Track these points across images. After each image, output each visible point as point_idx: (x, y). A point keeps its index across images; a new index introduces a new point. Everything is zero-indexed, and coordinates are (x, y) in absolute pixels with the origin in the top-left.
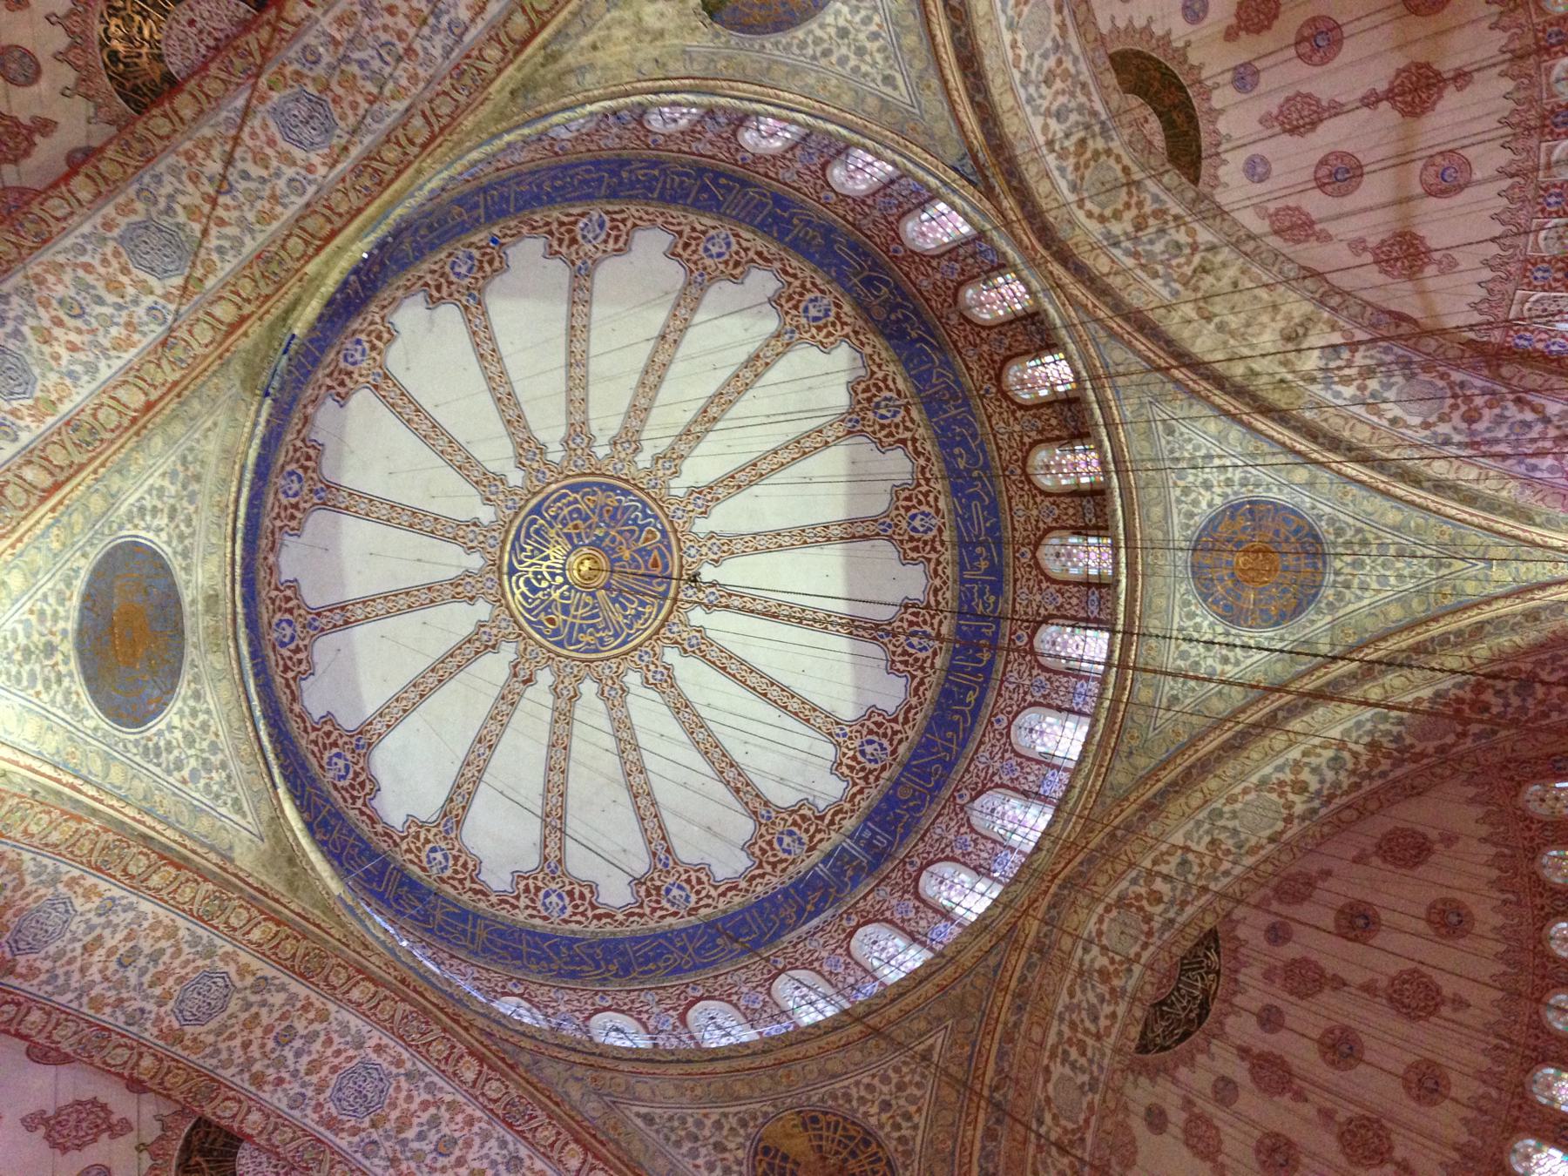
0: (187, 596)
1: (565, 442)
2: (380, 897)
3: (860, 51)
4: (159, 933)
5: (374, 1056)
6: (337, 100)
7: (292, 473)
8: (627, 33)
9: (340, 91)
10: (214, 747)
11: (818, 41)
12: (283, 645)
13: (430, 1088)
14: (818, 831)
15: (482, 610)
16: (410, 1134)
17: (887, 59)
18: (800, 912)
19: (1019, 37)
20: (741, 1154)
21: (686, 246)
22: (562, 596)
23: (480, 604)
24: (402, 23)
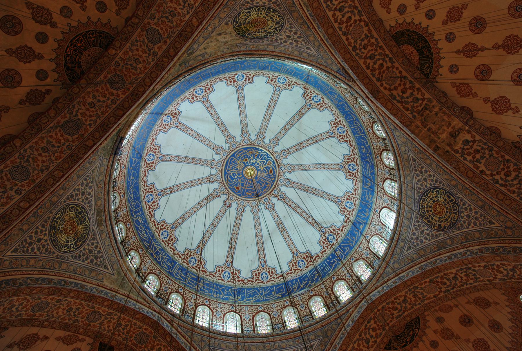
2: (170, 273)
4: (77, 304)
6: (125, 75)
9: (126, 73)
10: (99, 252)
11: (281, 39)
12: (149, 202)
13: (159, 340)
17: (306, 43)
19: (349, 37)
24: (141, 53)
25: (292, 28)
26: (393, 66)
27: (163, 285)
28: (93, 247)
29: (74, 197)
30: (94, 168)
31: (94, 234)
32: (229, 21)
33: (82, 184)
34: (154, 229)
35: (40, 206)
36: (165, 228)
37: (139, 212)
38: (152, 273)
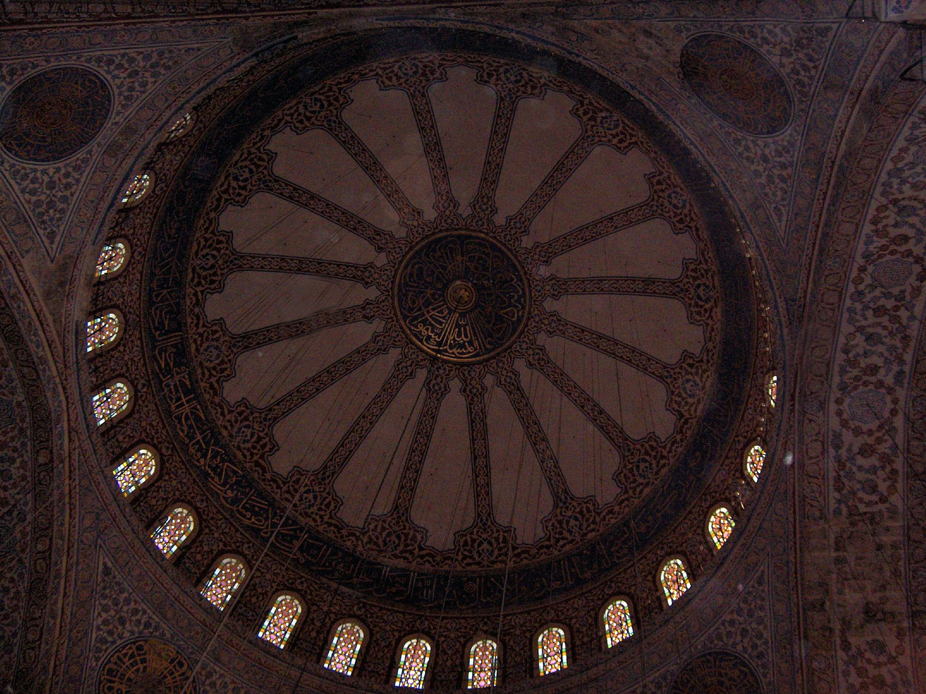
0: (114, 118)
1: (509, 219)
7: (316, 99)
8: (623, 41)
10: (64, 199)
11: (747, 149)
12: (236, 178)
13: (24, 445)
14: (411, 552)
19: (870, 268)
20: (127, 634)
21: (659, 183)
22: (433, 295)
23: (383, 255)
25: (788, 152)
27: (121, 348)
28: (64, 181)
29: (112, 67)
30: (196, 46)
31: (85, 161)
32: (688, 30)
33: (147, 57)
34: (198, 235)
35: (39, 32)
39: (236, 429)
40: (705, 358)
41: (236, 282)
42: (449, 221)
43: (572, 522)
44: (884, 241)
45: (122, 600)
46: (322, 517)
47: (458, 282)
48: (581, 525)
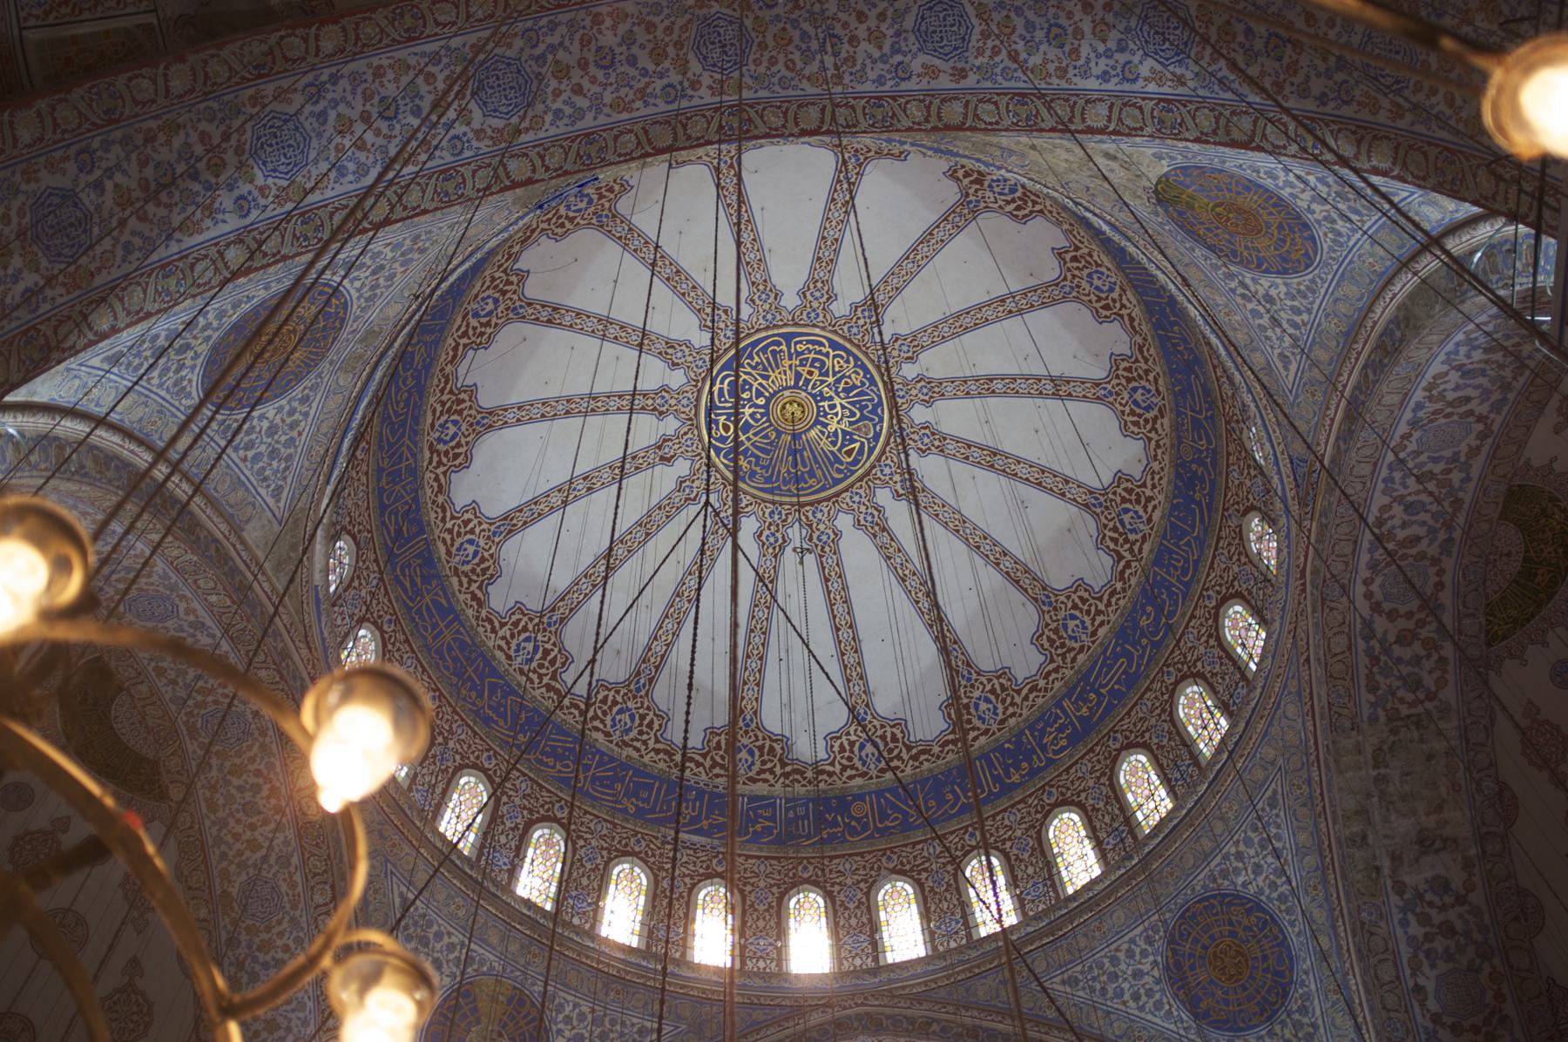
3: (1275, 322)
5: (250, 716)
6: (763, 46)
9: (771, 43)
12: (476, 315)
14: (771, 771)
15: (677, 379)
16: (236, 782)
18: (695, 820)
19: (1416, 435)
22: (752, 415)
24: (862, 32)
25: (1305, 297)
26: (1439, 560)
27: (356, 583)
28: (288, 421)
34: (432, 400)
36: (460, 413)
37: (431, 332)
38: (349, 533)
39: (513, 647)
40: (1149, 483)
41: (489, 447)
42: (769, 317)
43: (983, 706)
44: (1438, 406)
45: (431, 936)
46: (645, 743)
47: (787, 393)
48: (995, 708)
